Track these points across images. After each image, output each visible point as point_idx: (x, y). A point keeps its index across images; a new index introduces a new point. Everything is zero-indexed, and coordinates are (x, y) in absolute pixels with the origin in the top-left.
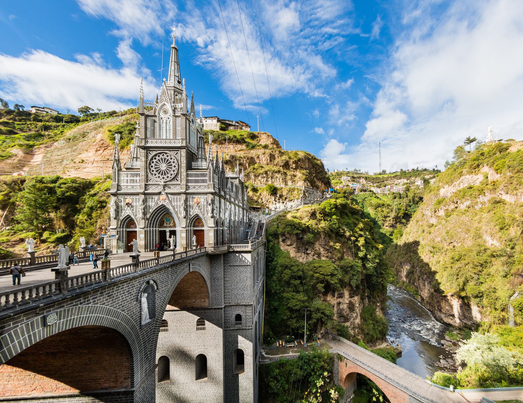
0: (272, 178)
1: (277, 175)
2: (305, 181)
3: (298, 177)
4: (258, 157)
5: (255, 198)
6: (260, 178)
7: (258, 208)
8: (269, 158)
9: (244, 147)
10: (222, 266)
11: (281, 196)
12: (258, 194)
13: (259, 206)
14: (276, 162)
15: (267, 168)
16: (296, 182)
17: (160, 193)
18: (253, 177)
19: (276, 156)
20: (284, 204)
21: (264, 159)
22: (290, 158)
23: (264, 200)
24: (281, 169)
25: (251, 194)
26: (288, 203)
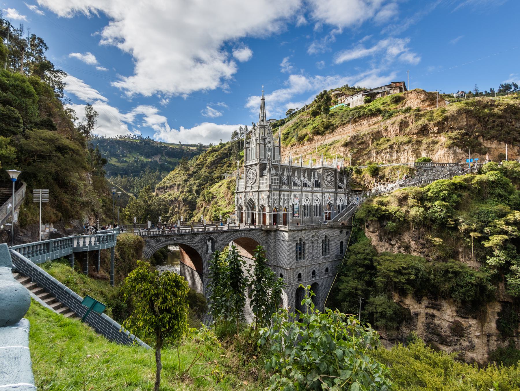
0: (397, 151)
1: (405, 147)
2: (449, 148)
3: (440, 143)
4: (386, 130)
5: (358, 180)
6: (382, 154)
7: (360, 191)
8: (398, 128)
9: (380, 118)
10: (273, 239)
11: (382, 177)
12: (362, 176)
13: (360, 189)
14: (408, 130)
15: (393, 140)
16: (435, 151)
17: (249, 192)
18: (374, 155)
19: (410, 123)
20: (386, 186)
21: (392, 131)
22: (430, 120)
23: (366, 183)
24: (415, 137)
25: (355, 176)
26: (389, 185)
